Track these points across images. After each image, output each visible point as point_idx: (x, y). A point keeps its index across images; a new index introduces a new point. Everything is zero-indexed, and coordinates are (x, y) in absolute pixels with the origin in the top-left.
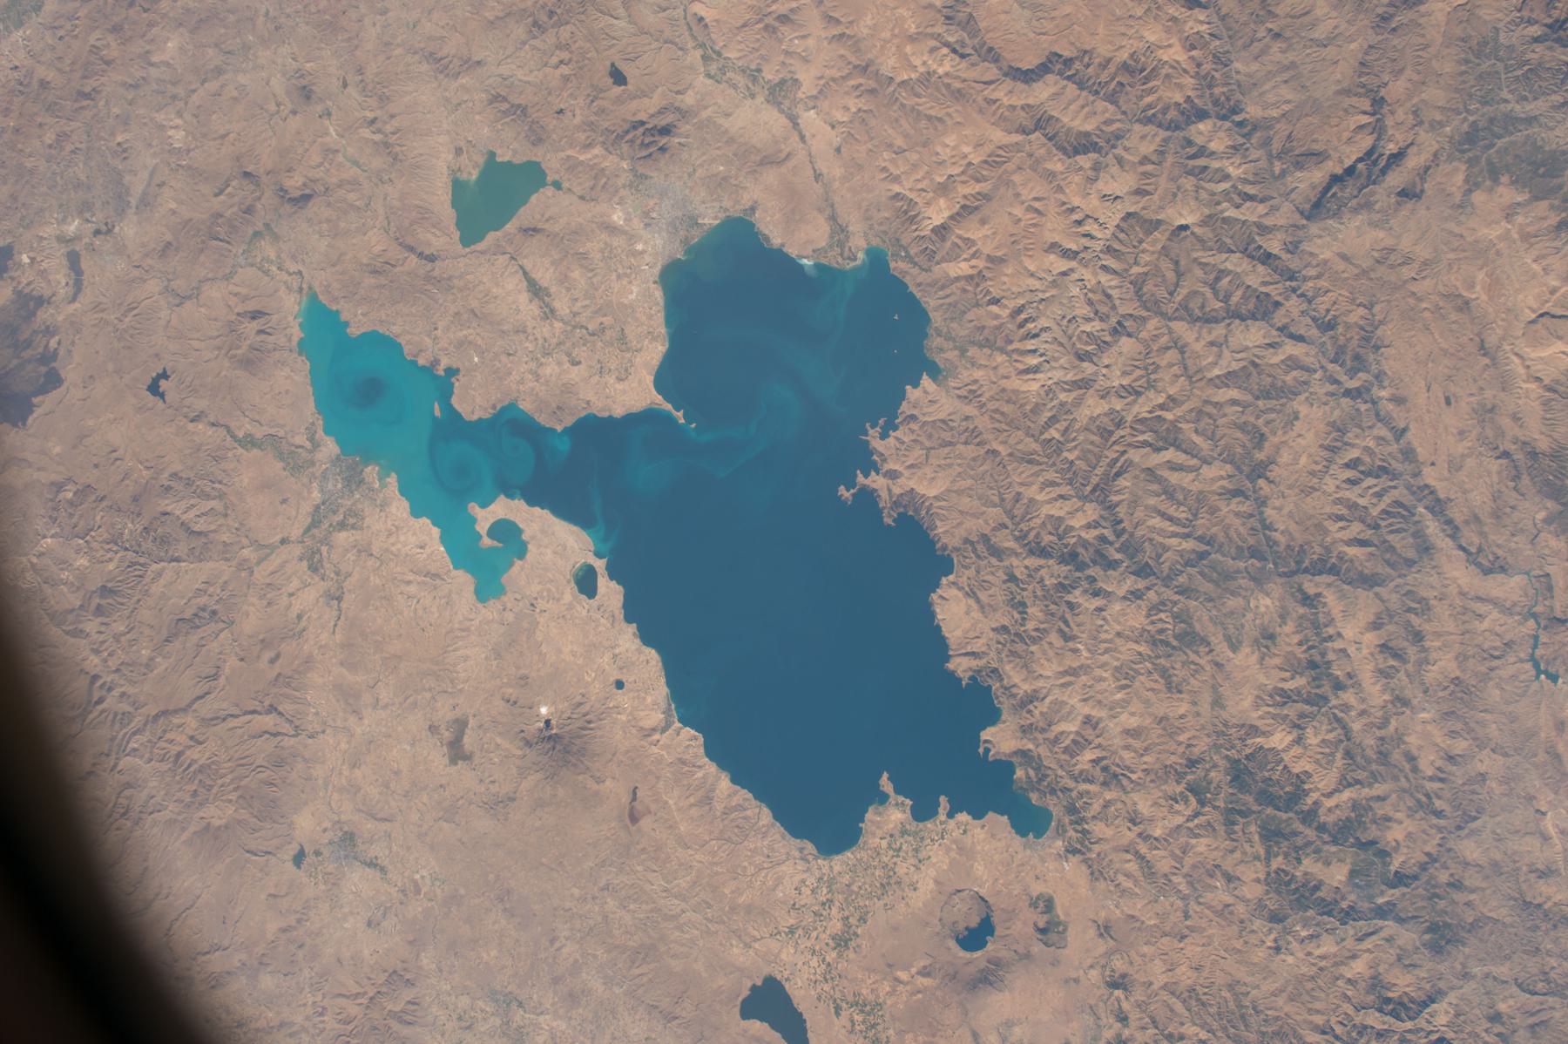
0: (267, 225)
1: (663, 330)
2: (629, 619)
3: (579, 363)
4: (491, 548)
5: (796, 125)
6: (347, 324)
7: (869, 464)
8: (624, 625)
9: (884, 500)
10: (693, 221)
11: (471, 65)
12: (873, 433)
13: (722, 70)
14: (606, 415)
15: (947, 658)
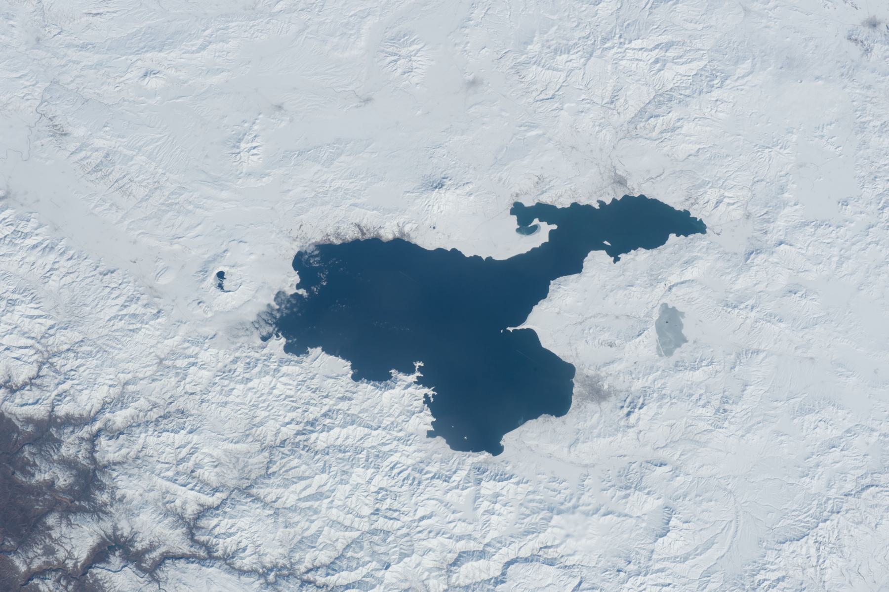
4: (532, 221)
7: (420, 381)
9: (401, 376)
15: (323, 350)
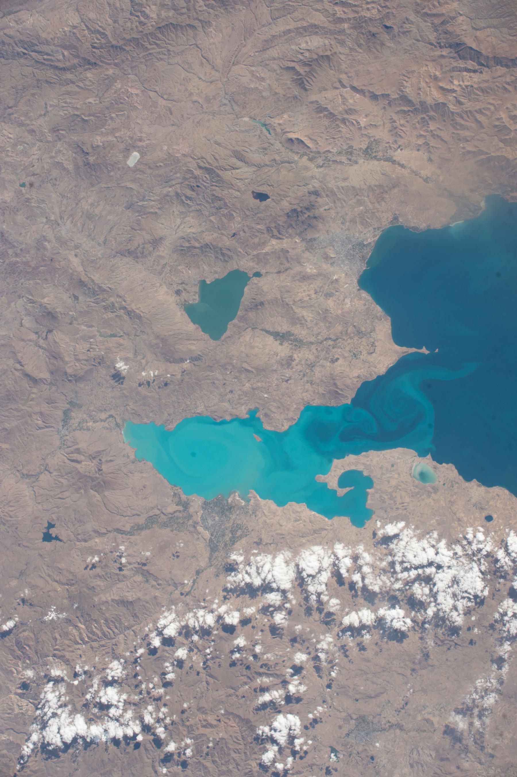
0: (71, 403)
2: (468, 478)
3: (338, 359)
5: (394, 162)
8: (467, 484)
10: (361, 245)
11: (157, 242)
13: (326, 159)
14: (375, 377)
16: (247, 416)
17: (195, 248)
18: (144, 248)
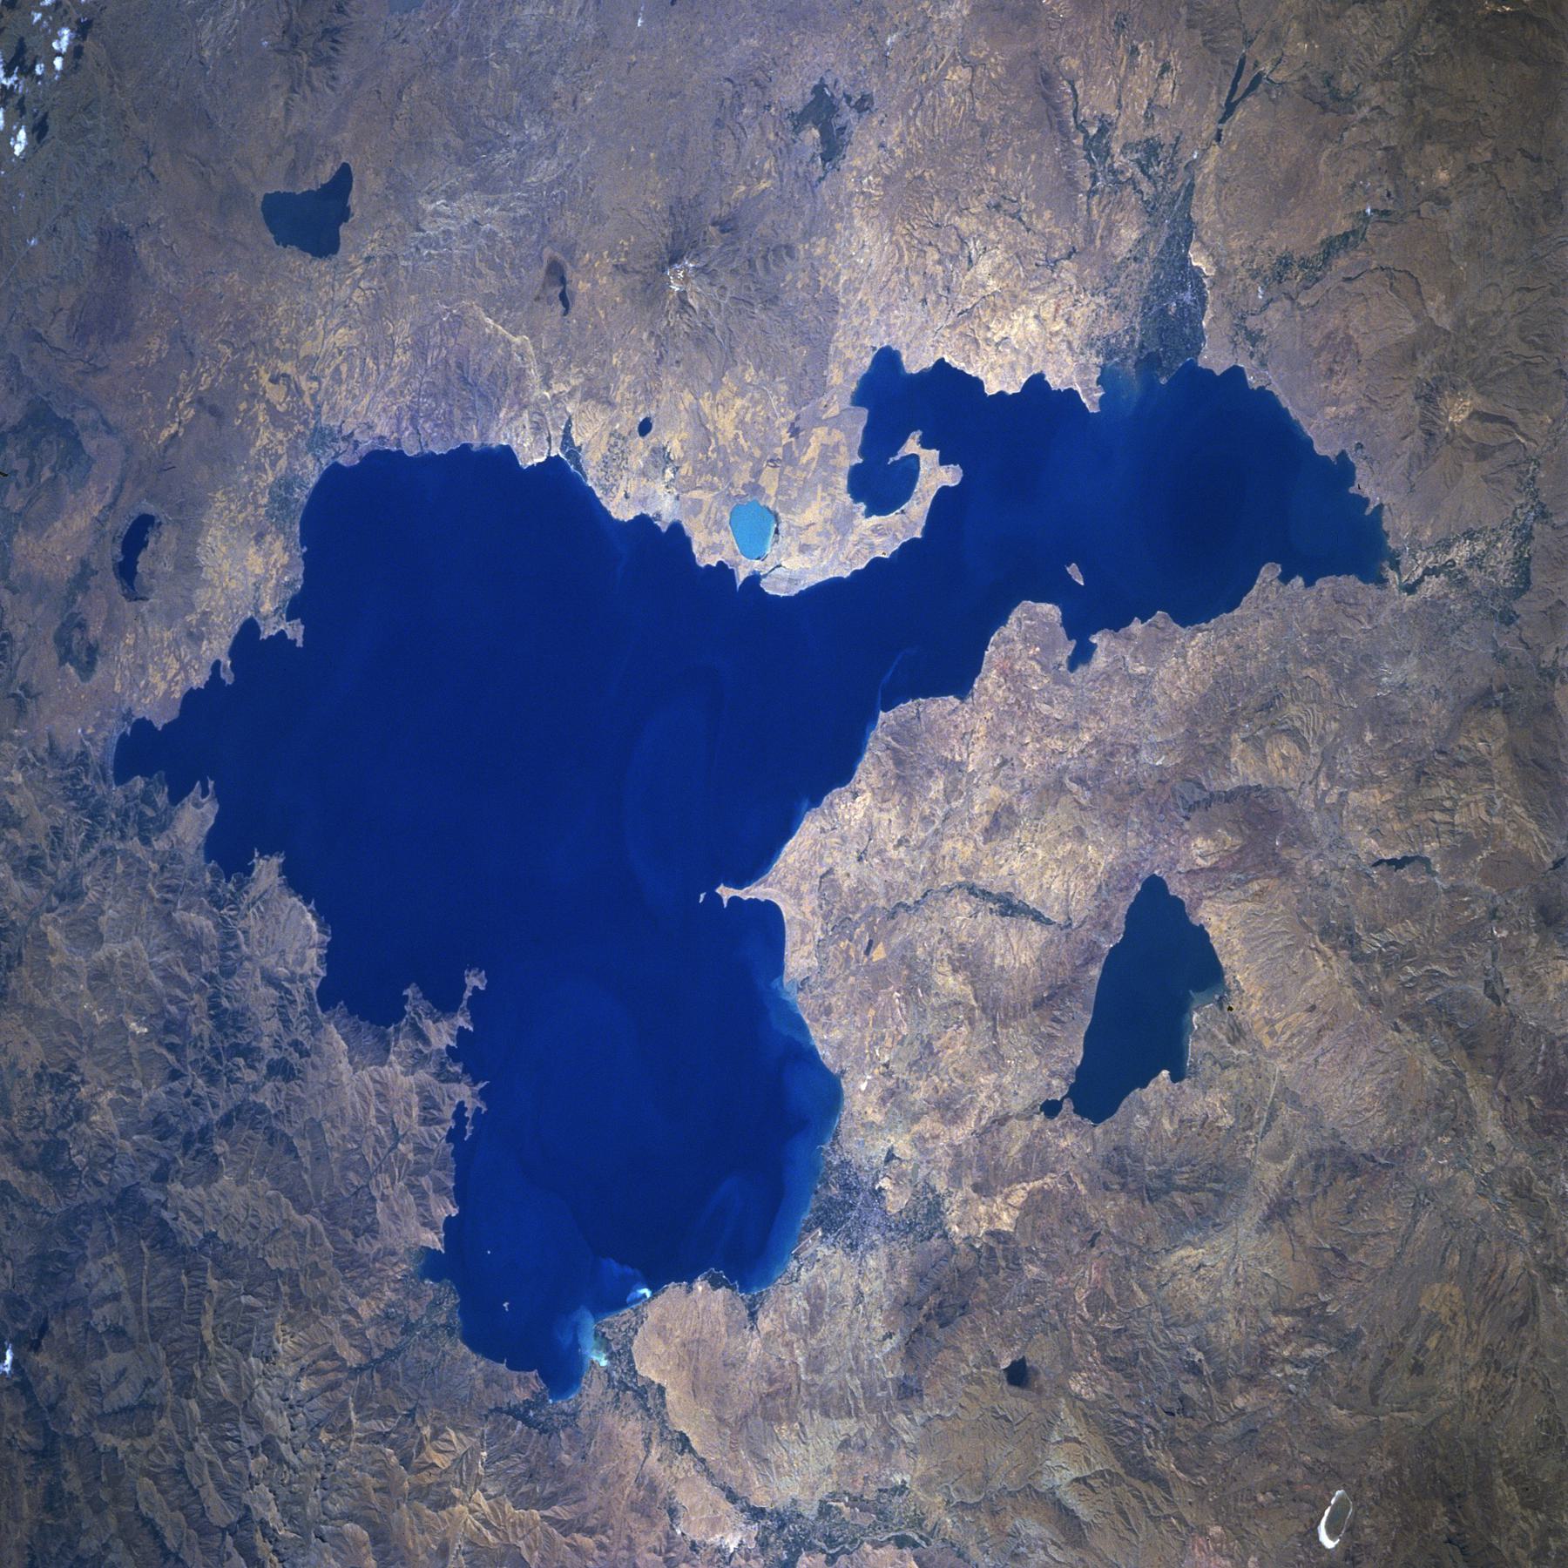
1: (805, 1005)
6: (1285, 578)
10: (830, 1220)
12: (471, 1104)
16: (1094, 640)
17: (1184, 1189)
18: (1314, 1184)
